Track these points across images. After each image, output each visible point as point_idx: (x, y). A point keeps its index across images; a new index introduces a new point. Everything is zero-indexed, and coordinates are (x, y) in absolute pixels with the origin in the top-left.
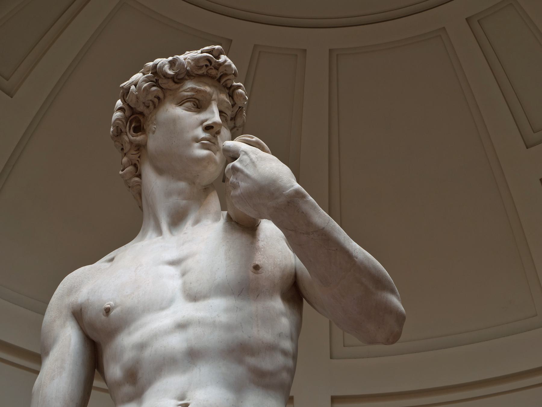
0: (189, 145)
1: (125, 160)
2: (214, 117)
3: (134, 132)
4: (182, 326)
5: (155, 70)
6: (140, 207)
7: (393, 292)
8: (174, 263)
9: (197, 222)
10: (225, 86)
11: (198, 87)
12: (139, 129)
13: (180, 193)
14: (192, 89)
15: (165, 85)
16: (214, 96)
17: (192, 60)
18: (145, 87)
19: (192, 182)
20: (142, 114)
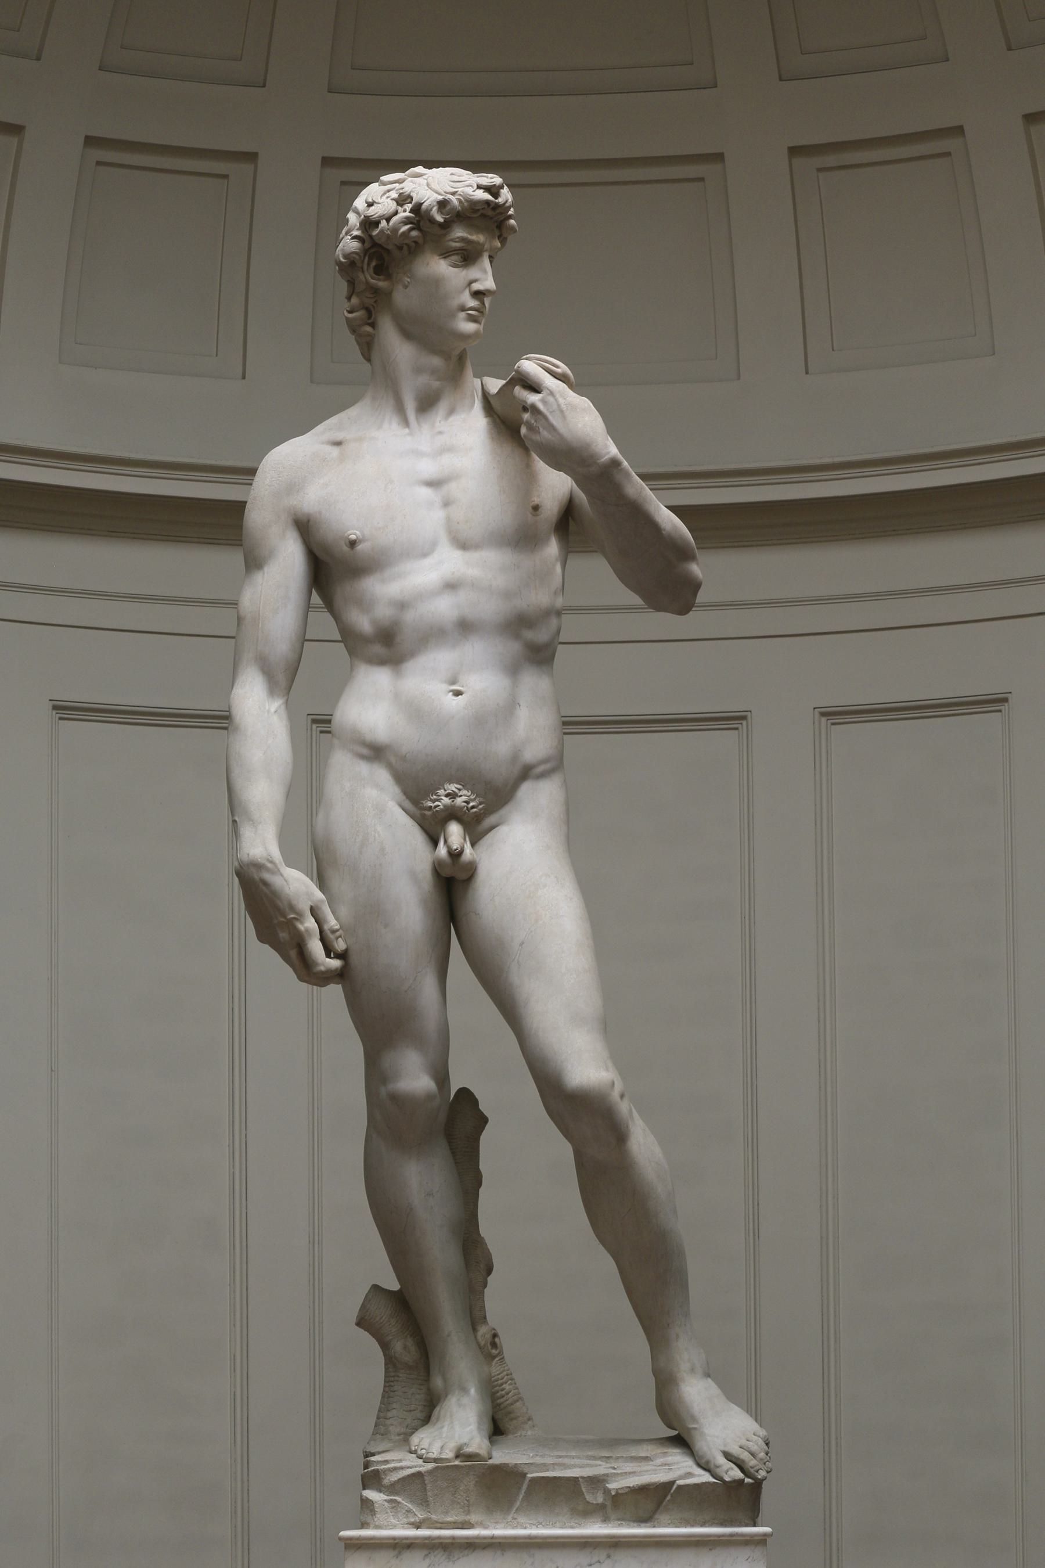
0: (452, 315)
1: (355, 300)
2: (486, 280)
3: (375, 273)
4: (451, 586)
5: (417, 209)
6: (363, 355)
7: (692, 557)
8: (434, 484)
9: (451, 411)
11: (470, 237)
12: (381, 270)
13: (433, 372)
14: (463, 240)
15: (428, 228)
16: (487, 246)
17: (467, 201)
18: (404, 233)
19: (446, 355)
20: (388, 251)
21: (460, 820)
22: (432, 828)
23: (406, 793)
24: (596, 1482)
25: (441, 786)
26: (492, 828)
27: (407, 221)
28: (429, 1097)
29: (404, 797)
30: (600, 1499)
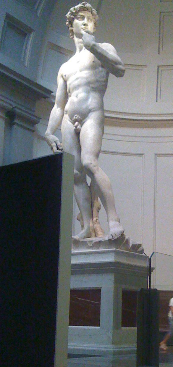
0: (80, 30)
4: (77, 79)
5: (71, 11)
8: (78, 62)
10: (89, 12)
14: (80, 15)
16: (85, 16)
21: (77, 121)
22: (74, 123)
23: (70, 119)
24: (91, 242)
25: (74, 116)
26: (84, 122)
27: (70, 14)
28: (77, 174)
29: (70, 119)
30: (92, 245)
